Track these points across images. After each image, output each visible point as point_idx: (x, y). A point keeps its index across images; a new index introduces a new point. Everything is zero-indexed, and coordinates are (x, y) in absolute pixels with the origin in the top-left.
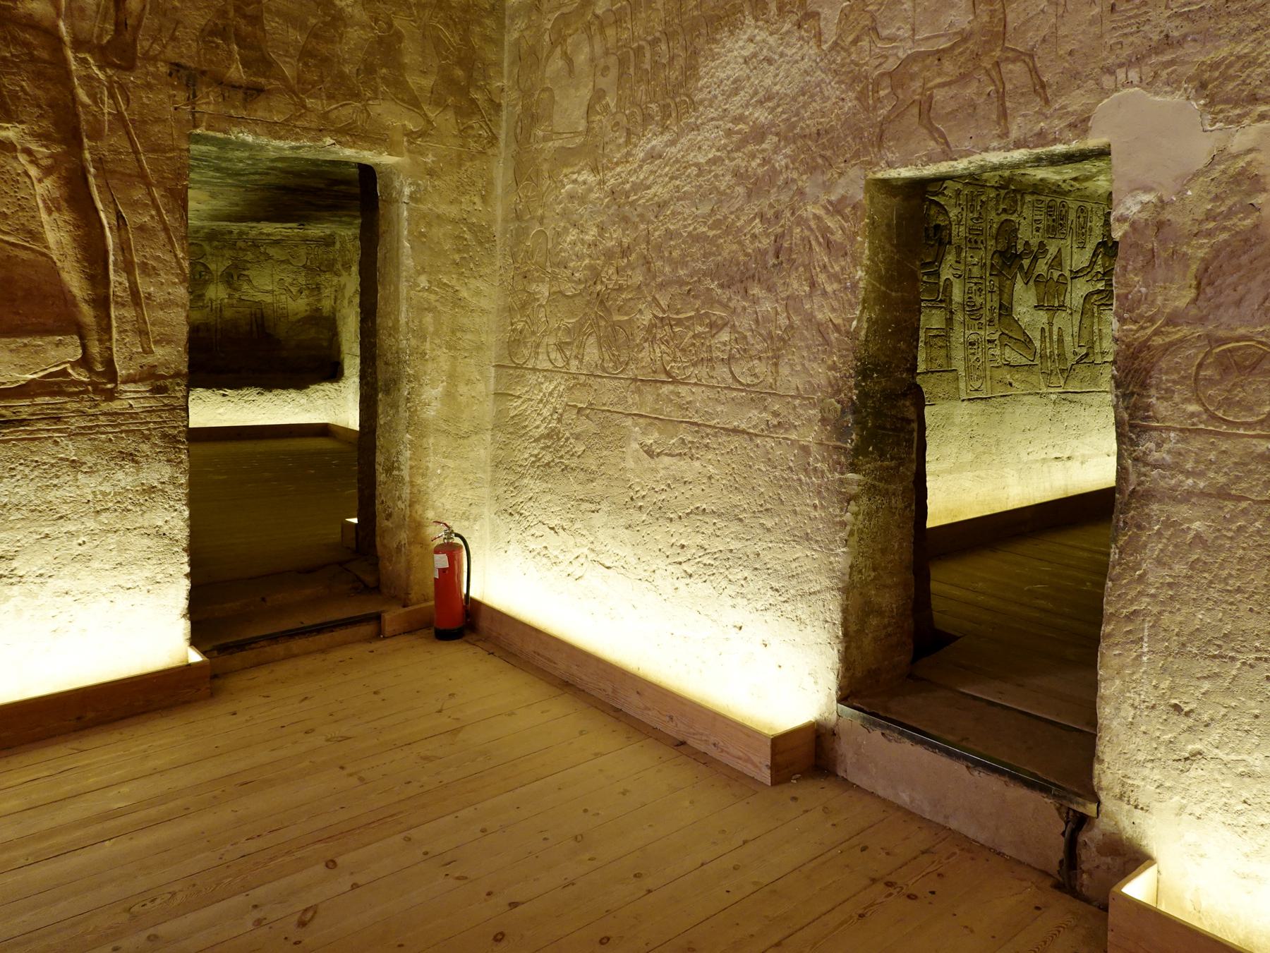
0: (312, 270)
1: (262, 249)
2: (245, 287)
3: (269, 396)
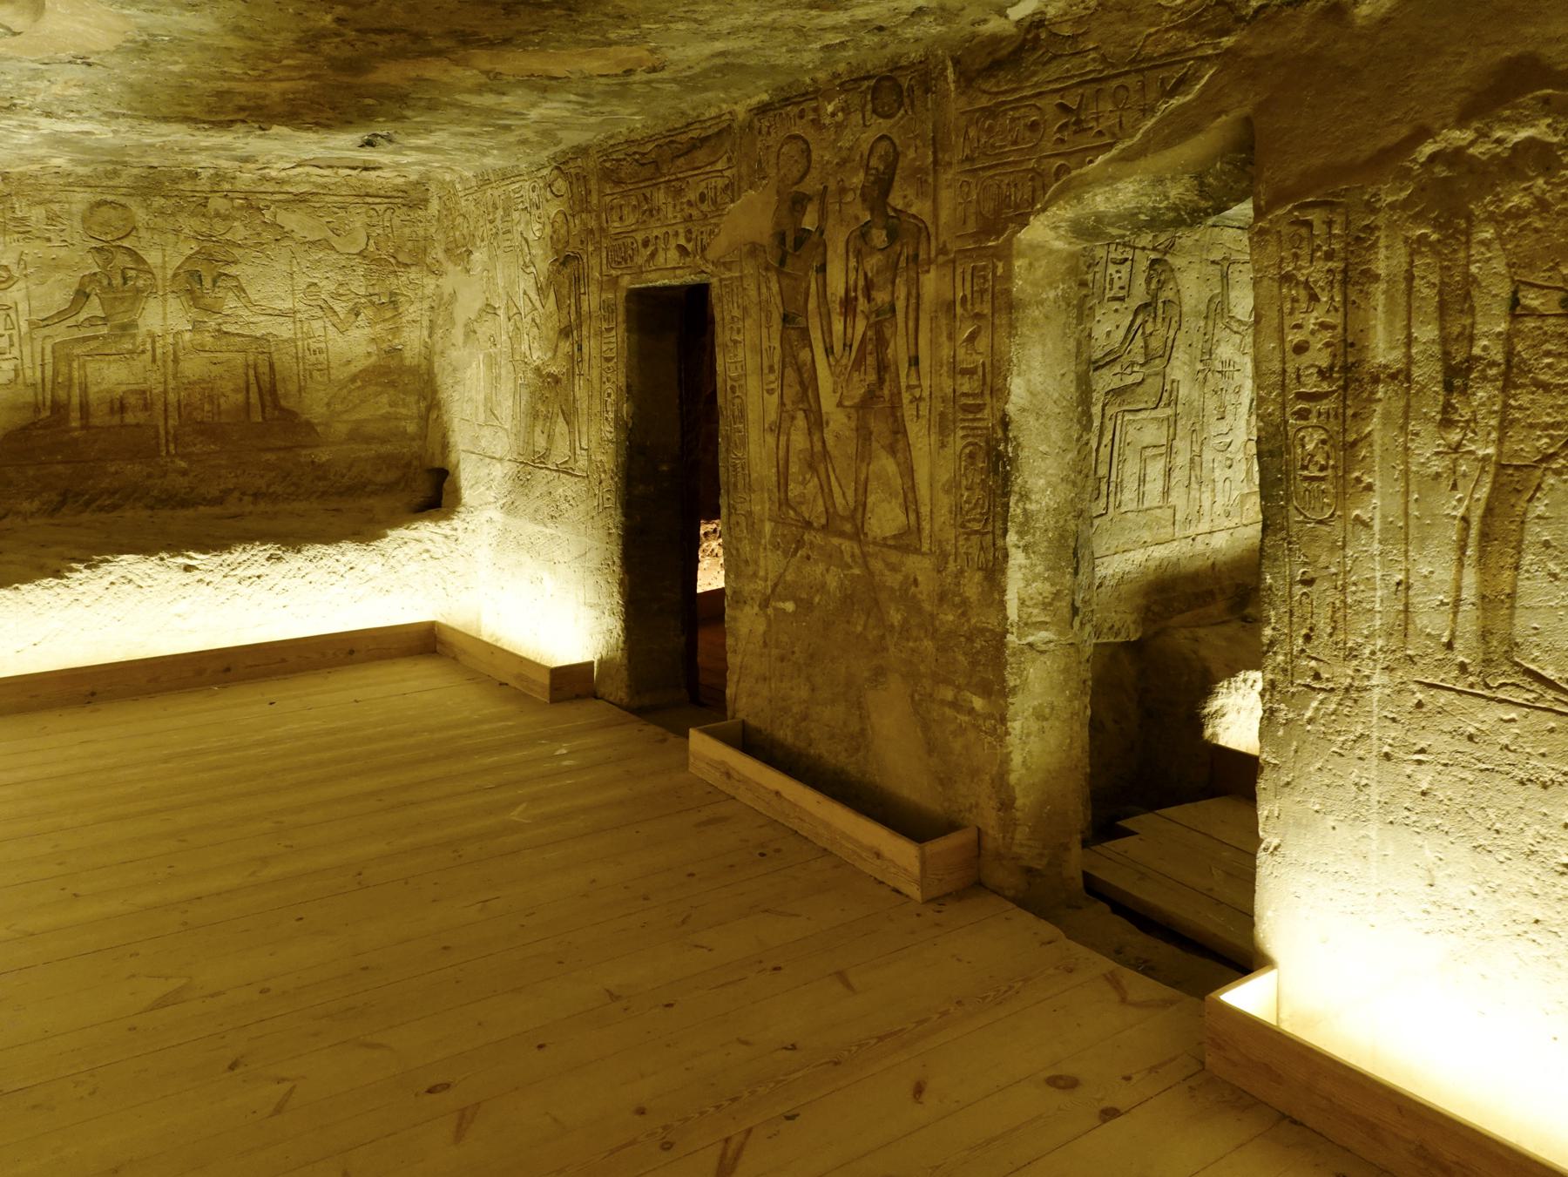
0: (378, 261)
1: (268, 216)
2: (231, 303)
3: (295, 561)
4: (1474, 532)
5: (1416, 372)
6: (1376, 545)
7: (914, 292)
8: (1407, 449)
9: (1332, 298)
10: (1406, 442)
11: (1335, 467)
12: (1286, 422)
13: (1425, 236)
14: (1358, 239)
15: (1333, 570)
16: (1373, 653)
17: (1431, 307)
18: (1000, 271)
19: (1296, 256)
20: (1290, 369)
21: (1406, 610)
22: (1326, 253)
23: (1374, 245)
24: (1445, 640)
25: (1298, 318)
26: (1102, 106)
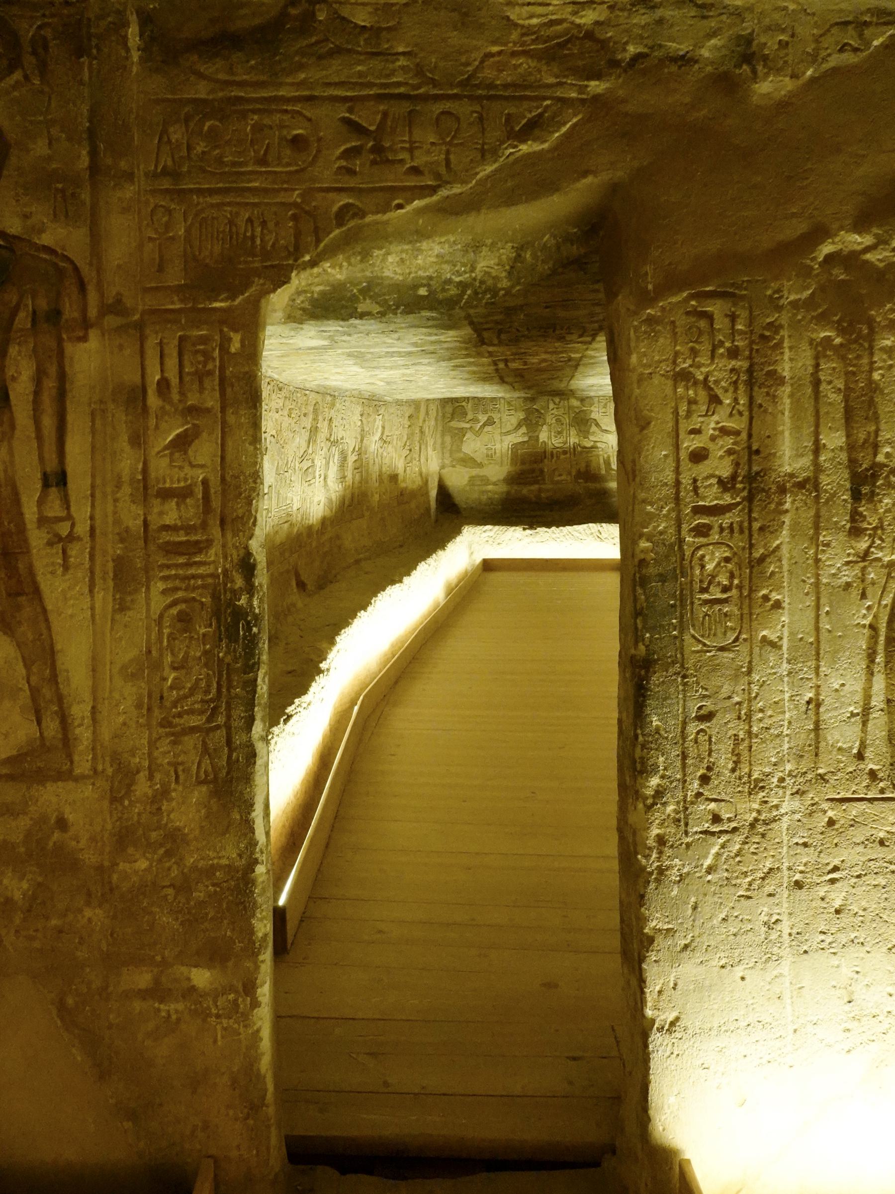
4: (882, 639)
5: (824, 480)
6: (785, 665)
7: (53, 370)
8: (817, 561)
9: (736, 400)
10: (816, 553)
11: (740, 587)
12: (681, 541)
13: (828, 339)
14: (762, 337)
15: (737, 699)
16: (782, 780)
17: (839, 415)
18: (235, 346)
19: (694, 352)
20: (686, 480)
21: (817, 728)
22: (728, 350)
23: (779, 345)
24: (855, 751)
25: (696, 421)
26: (417, 134)
